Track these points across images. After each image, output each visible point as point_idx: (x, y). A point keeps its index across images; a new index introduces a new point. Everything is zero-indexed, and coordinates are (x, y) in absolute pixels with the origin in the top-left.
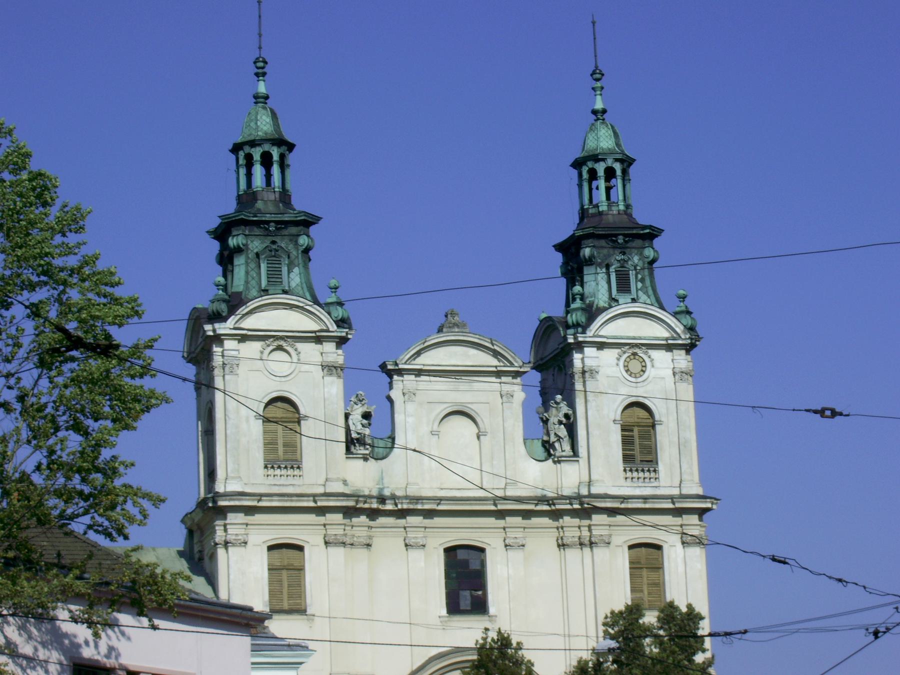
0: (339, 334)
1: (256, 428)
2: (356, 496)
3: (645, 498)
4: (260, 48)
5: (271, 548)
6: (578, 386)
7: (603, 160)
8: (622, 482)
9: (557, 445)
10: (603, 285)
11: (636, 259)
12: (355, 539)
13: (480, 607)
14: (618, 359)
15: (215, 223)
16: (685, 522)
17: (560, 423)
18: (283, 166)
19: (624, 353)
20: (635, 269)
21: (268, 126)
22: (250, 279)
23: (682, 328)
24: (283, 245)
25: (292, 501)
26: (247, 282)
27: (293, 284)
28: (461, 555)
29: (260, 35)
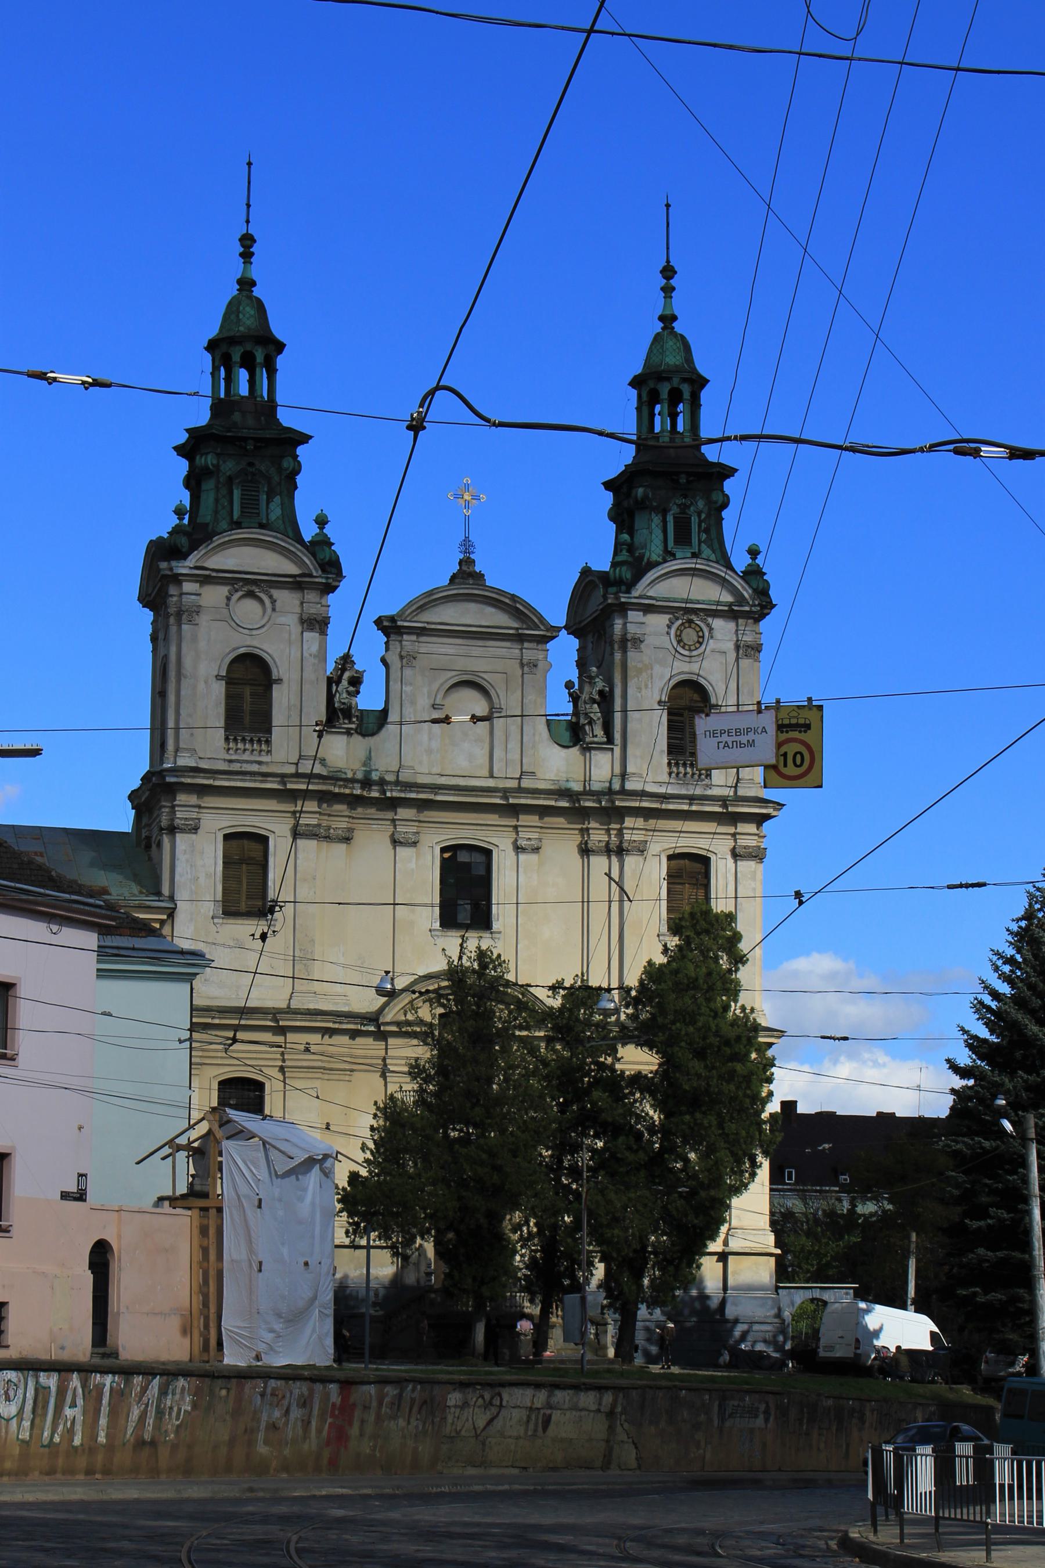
0: (324, 581)
1: (219, 689)
2: (333, 778)
3: (692, 799)
4: (248, 222)
5: (227, 837)
6: (618, 656)
7: (669, 379)
8: (665, 778)
9: (587, 728)
10: (658, 533)
11: (701, 504)
12: (332, 831)
13: (482, 920)
14: (669, 627)
15: (183, 438)
16: (738, 830)
17: (594, 701)
18: (272, 371)
20: (699, 516)
21: (252, 320)
22: (220, 507)
23: (750, 591)
24: (263, 468)
25: (255, 781)
26: (216, 512)
27: (273, 517)
28: (463, 857)
29: (248, 206)
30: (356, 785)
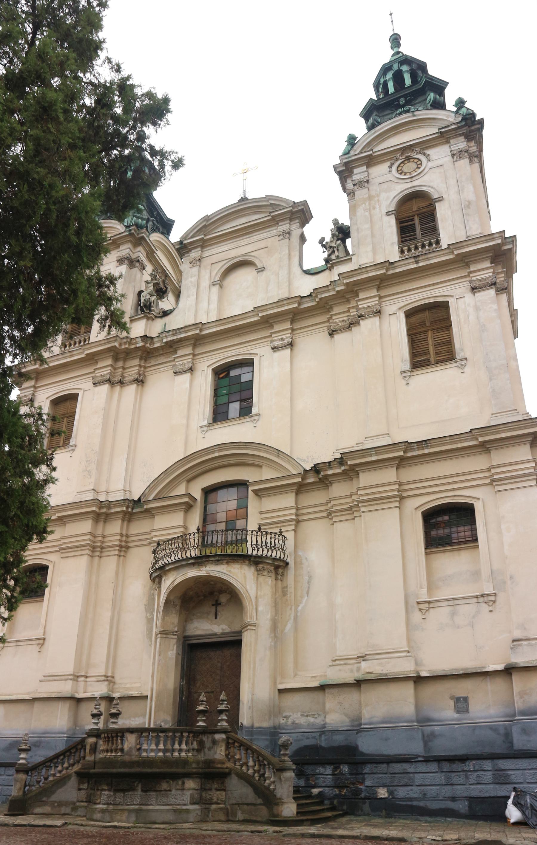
14: (390, 167)
19: (397, 160)
30: (138, 340)
